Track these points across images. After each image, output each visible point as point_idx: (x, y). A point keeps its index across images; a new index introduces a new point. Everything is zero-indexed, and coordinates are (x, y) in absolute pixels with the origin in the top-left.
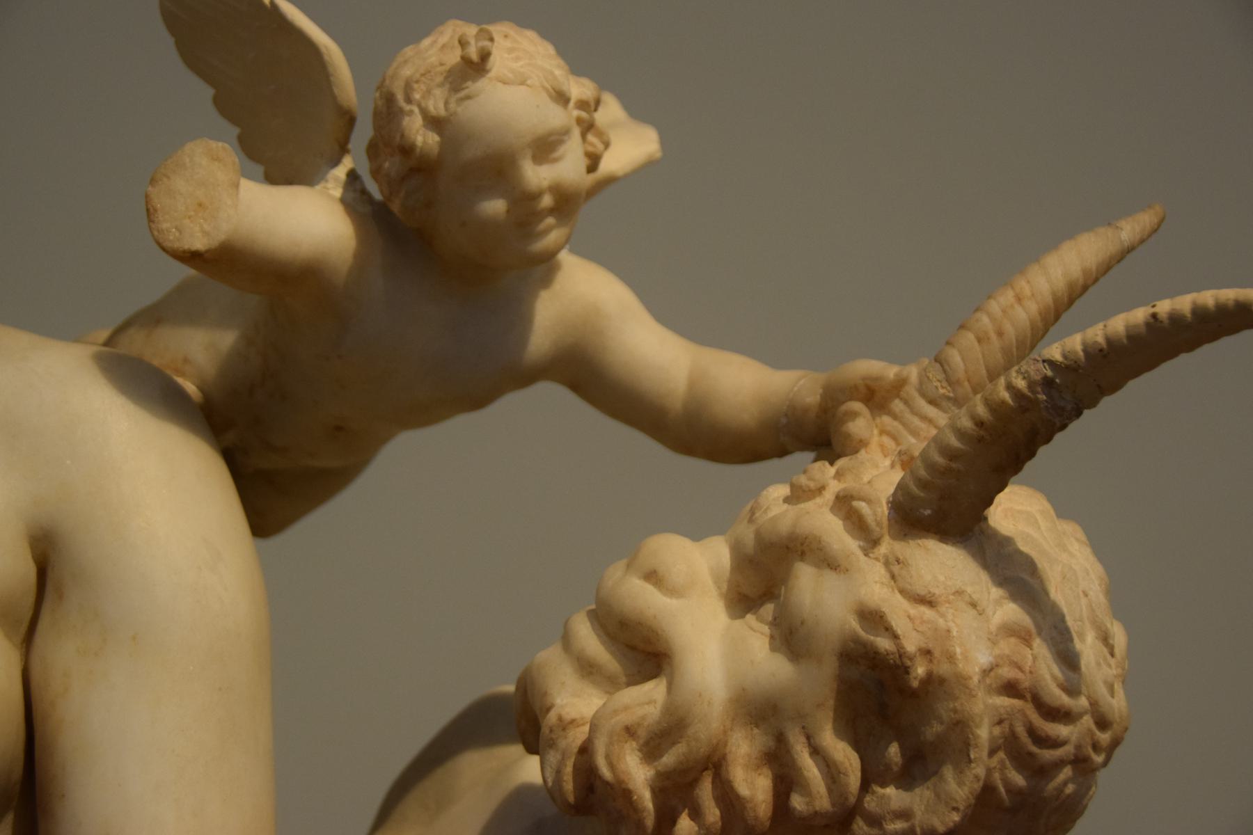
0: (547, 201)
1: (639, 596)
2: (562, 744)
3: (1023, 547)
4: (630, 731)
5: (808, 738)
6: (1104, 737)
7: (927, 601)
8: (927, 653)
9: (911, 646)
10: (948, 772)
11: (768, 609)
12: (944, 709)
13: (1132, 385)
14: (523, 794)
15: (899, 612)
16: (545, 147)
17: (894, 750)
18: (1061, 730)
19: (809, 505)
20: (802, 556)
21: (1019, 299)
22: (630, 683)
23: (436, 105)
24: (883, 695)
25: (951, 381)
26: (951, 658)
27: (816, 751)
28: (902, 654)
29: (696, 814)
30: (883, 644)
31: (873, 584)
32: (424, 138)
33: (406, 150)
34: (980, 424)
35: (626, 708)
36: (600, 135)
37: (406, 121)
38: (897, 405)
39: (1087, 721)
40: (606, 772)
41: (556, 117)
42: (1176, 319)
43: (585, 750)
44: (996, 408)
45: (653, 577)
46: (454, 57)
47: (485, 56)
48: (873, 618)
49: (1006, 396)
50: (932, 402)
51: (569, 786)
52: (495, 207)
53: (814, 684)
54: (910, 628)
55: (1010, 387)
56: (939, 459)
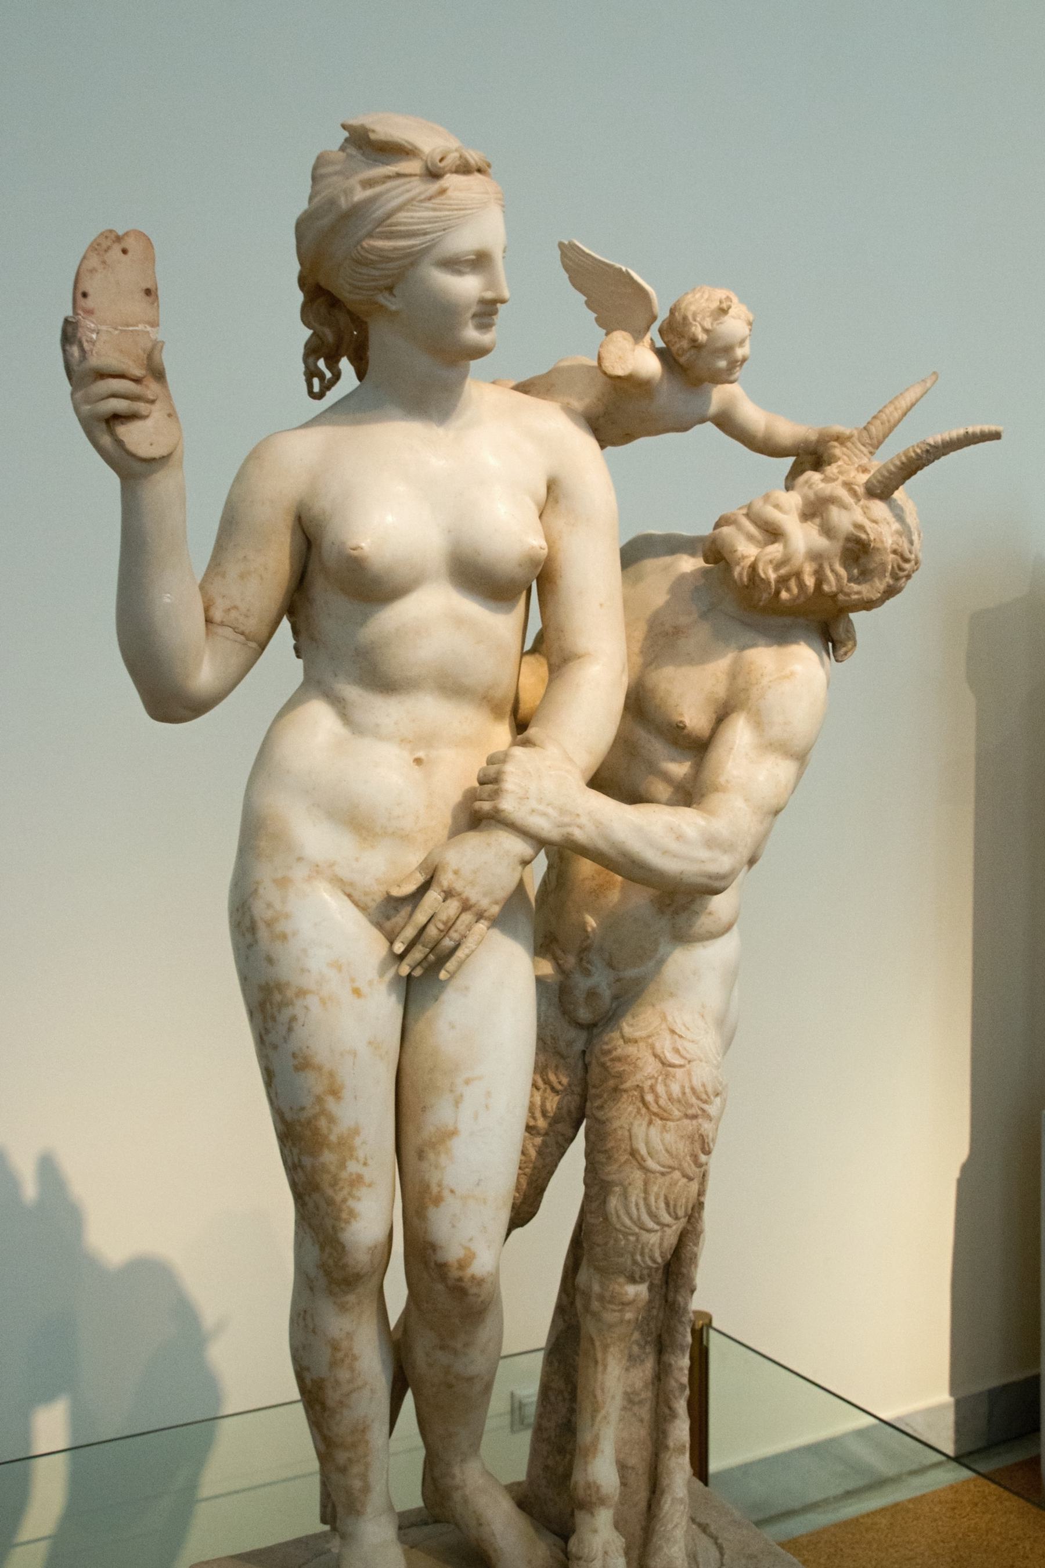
1: (772, 514)
2: (742, 564)
4: (771, 561)
5: (831, 566)
7: (875, 522)
10: (876, 580)
11: (817, 521)
12: (877, 559)
13: (952, 454)
14: (683, 577)
15: (868, 524)
17: (856, 571)
18: (907, 566)
19: (833, 484)
20: (833, 503)
21: (896, 409)
22: (766, 544)
23: (708, 324)
25: (871, 438)
26: (882, 542)
27: (833, 571)
28: (869, 541)
29: (788, 590)
30: (863, 536)
32: (702, 337)
34: (903, 463)
35: (771, 553)
37: (693, 329)
39: (913, 563)
40: (763, 575)
42: (974, 435)
43: (753, 567)
45: (777, 506)
46: (715, 305)
47: (729, 307)
48: (860, 527)
49: (913, 454)
50: (864, 445)
51: (745, 579)
54: (872, 532)
55: (914, 451)
56: (886, 474)
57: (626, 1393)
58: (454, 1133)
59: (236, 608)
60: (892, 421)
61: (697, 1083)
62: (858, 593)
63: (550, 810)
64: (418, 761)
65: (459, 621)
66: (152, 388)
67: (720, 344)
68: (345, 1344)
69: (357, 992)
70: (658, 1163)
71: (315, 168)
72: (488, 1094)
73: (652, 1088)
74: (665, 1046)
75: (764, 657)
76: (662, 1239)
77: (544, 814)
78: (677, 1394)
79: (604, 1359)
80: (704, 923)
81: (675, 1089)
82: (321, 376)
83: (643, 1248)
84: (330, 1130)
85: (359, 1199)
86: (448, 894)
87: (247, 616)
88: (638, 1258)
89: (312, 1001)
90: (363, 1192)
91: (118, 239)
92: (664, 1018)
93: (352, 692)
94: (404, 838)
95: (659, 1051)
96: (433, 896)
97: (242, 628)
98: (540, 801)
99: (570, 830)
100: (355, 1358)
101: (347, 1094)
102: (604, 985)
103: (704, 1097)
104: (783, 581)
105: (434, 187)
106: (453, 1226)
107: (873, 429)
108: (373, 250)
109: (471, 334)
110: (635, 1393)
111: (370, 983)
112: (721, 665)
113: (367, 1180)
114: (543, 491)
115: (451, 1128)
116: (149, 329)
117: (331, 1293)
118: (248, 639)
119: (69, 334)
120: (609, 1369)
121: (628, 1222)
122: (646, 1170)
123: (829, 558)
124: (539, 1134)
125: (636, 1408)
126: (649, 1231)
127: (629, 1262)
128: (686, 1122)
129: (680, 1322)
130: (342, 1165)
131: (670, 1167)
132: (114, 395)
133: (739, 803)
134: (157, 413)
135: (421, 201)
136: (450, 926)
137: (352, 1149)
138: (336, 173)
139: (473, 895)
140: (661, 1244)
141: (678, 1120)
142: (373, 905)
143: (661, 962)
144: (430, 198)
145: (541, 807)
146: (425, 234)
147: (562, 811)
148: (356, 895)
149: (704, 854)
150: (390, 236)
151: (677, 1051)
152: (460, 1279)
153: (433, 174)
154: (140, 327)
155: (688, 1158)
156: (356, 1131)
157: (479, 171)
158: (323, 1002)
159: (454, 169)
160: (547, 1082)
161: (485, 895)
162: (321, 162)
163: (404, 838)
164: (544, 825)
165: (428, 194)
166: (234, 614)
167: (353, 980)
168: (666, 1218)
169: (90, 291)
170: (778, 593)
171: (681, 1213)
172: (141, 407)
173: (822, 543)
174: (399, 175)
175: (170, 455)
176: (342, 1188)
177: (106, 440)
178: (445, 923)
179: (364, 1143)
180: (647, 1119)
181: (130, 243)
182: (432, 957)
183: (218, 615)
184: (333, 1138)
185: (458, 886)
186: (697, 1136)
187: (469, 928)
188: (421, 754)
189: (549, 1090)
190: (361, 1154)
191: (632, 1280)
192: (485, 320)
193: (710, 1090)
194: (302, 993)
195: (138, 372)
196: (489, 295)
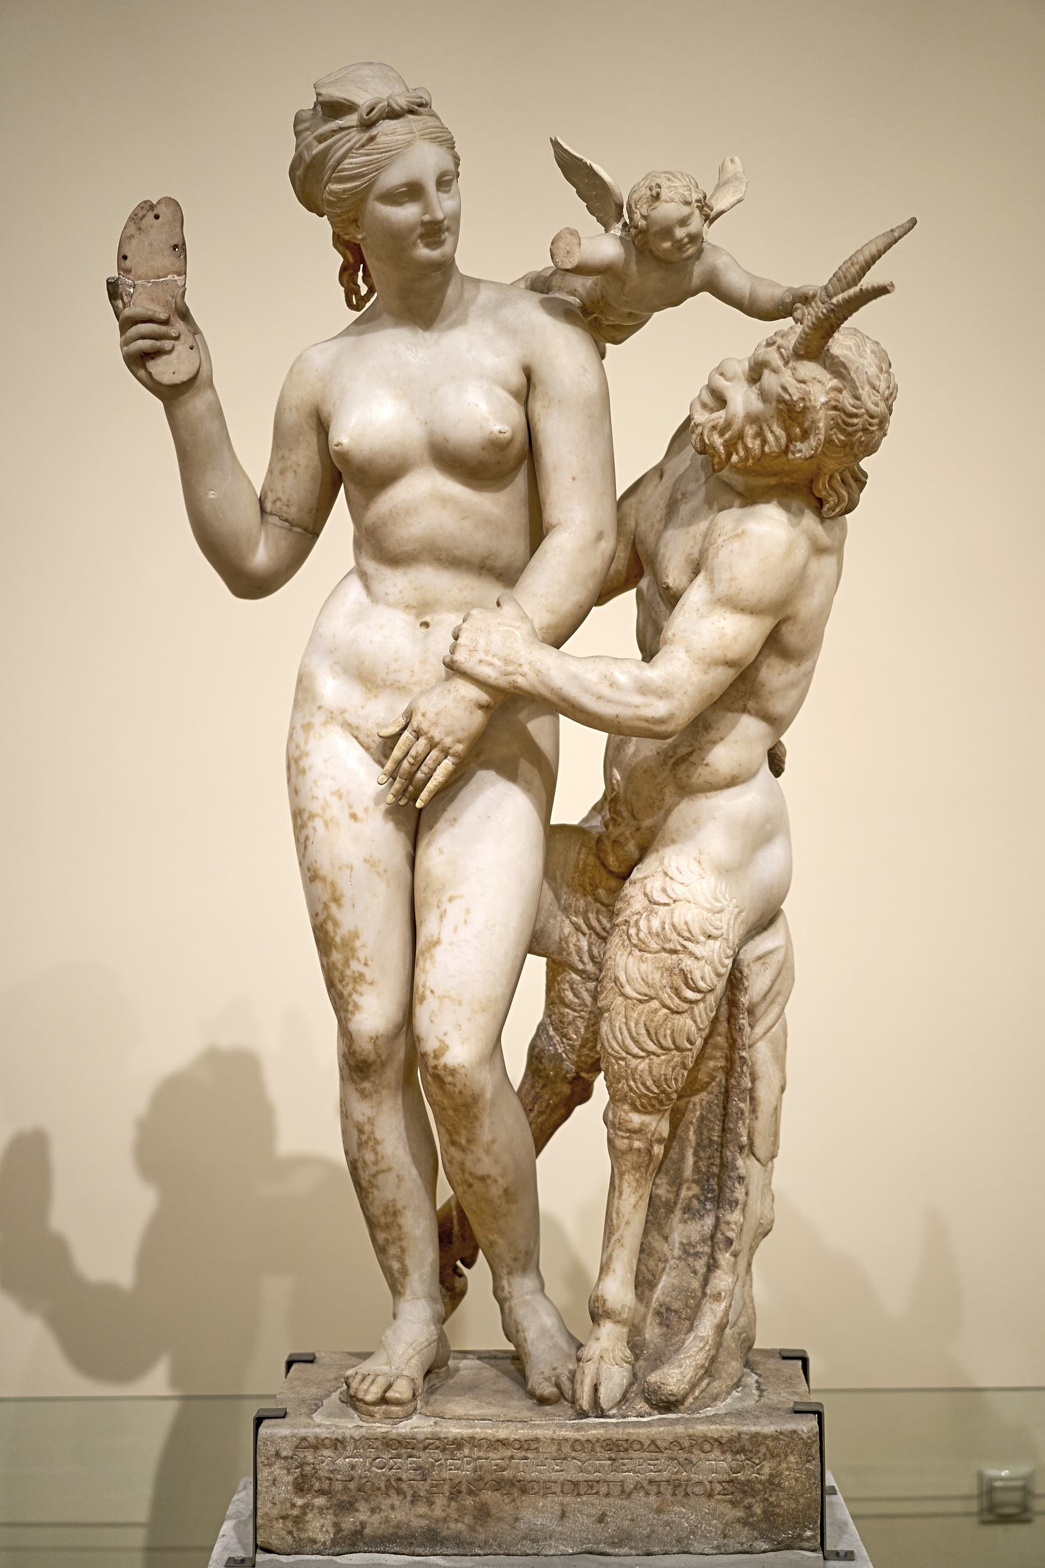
0: (686, 240)
3: (842, 359)
4: (714, 428)
6: (876, 421)
7: (803, 382)
8: (803, 399)
9: (795, 398)
10: (812, 437)
12: (809, 417)
16: (683, 222)
18: (855, 421)
21: (852, 264)
23: (644, 212)
24: (792, 413)
26: (810, 400)
27: (772, 432)
29: (737, 454)
30: (787, 397)
31: (787, 378)
32: (642, 223)
33: (636, 227)
36: (708, 207)
38: (813, 304)
39: (866, 417)
40: (707, 441)
41: (686, 210)
43: (702, 434)
44: (818, 318)
45: (722, 374)
46: (649, 193)
47: (658, 194)
48: (784, 389)
52: (667, 245)
57: (681, 1243)
58: (437, 943)
59: (279, 499)
60: (849, 276)
61: (676, 920)
62: (800, 451)
63: (495, 661)
64: (426, 625)
65: (445, 501)
67: (654, 229)
68: (367, 1128)
69: (354, 817)
70: (635, 990)
71: (295, 126)
72: (468, 911)
73: (637, 922)
74: (655, 886)
75: (728, 520)
77: (490, 664)
78: (721, 1246)
79: (620, 1186)
80: (700, 775)
81: (656, 924)
82: (357, 292)
83: (633, 1075)
84: (335, 932)
85: (362, 995)
86: (418, 734)
87: (288, 506)
88: (632, 1083)
89: (318, 823)
90: (364, 988)
91: (152, 207)
92: (662, 863)
93: (371, 566)
94: (400, 688)
95: (648, 891)
96: (406, 733)
97: (286, 516)
98: (487, 653)
99: (514, 678)
100: (377, 1142)
101: (346, 901)
102: (628, 833)
103: (687, 934)
104: (730, 447)
105: (366, 136)
106: (432, 1021)
107: (830, 287)
108: (331, 193)
109: (423, 252)
110: (690, 1244)
111: (366, 810)
112: (703, 526)
113: (369, 977)
114: (517, 379)
115: (435, 938)
116: (176, 278)
117: (354, 1082)
118: (292, 524)
119: (114, 290)
120: (624, 1196)
121: (617, 1048)
122: (626, 997)
123: (766, 420)
124: (590, 978)
125: (690, 1259)
126: (635, 1056)
127: (626, 1088)
128: (665, 955)
129: (730, 1177)
130: (346, 963)
131: (646, 995)
132: (143, 337)
133: (682, 655)
134: (181, 347)
135: (358, 149)
136: (419, 762)
137: (353, 950)
138: (307, 129)
139: (437, 734)
140: (650, 1072)
141: (657, 952)
142: (374, 746)
143: (668, 812)
144: (363, 146)
145: (489, 658)
146: (364, 176)
147: (507, 662)
148: (361, 737)
150: (341, 180)
151: (664, 890)
152: (435, 1067)
153: (367, 125)
154: (170, 277)
156: (355, 935)
157: (412, 112)
158: (326, 824)
159: (384, 115)
160: (591, 927)
161: (447, 734)
162: (298, 121)
163: (400, 688)
164: (489, 673)
165: (361, 142)
166: (278, 503)
167: (351, 807)
168: (652, 1047)
169: (129, 255)
170: (729, 456)
171: (668, 1043)
172: (167, 344)
173: (757, 405)
174: (342, 129)
176: (348, 984)
177: (142, 373)
178: (415, 758)
179: (364, 946)
180: (629, 950)
181: (162, 210)
182: (411, 788)
183: (269, 506)
184: (338, 939)
185: (425, 726)
186: (677, 971)
188: (427, 619)
189: (594, 936)
190: (361, 955)
191: (635, 1109)
192: (431, 240)
193: (696, 930)
194: (312, 816)
195: (163, 316)
196: (427, 218)
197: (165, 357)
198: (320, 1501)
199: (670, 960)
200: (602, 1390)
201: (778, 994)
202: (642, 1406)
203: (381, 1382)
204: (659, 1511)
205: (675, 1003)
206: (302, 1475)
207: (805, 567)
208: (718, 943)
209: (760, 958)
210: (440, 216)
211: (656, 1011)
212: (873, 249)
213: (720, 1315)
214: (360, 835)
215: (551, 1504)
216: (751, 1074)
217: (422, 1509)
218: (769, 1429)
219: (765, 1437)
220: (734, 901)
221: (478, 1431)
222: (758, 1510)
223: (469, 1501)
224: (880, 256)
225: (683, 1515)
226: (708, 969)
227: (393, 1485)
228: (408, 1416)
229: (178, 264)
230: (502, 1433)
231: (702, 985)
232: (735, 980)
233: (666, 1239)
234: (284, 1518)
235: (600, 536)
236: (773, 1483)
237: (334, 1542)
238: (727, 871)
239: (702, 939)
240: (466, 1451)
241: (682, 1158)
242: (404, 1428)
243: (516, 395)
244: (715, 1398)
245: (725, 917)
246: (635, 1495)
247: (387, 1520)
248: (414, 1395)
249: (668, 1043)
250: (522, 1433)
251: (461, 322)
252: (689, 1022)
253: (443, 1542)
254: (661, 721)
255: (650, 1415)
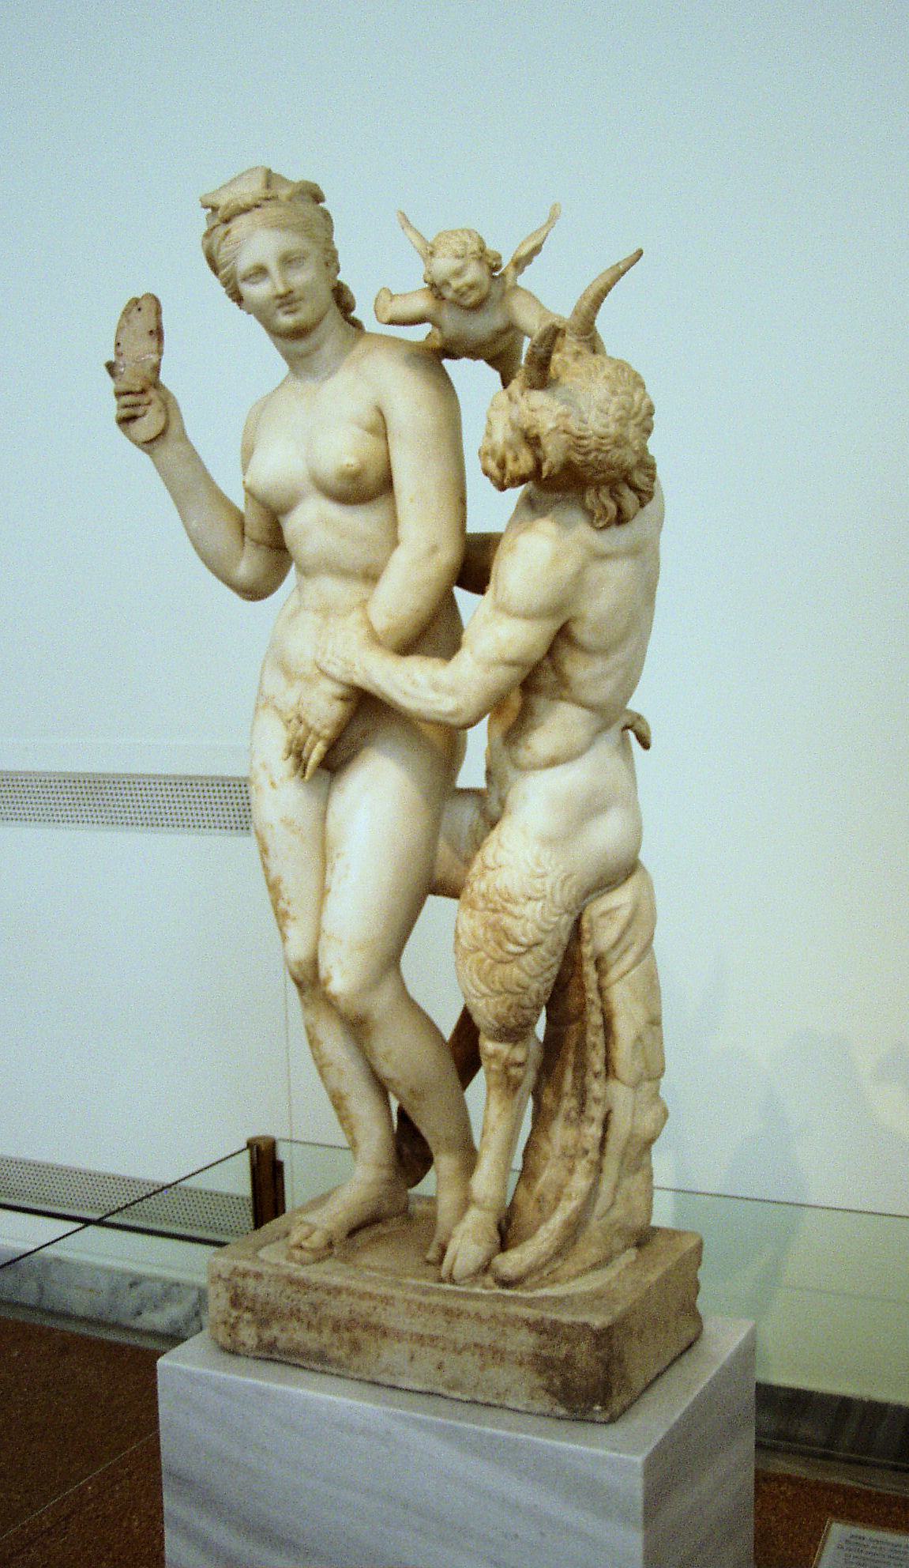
16: (458, 273)
18: (585, 442)
41: (458, 263)
53: (516, 438)
61: (498, 883)
66: (152, 394)
69: (273, 784)
76: (487, 1005)
90: (289, 922)
101: (271, 853)
114: (370, 417)
119: (111, 367)
134: (152, 411)
139: (311, 720)
149: (432, 696)
153: (227, 221)
155: (492, 943)
157: (258, 206)
168: (483, 988)
171: (498, 986)
172: (140, 411)
175: (163, 433)
181: (144, 304)
187: (314, 746)
190: (286, 896)
193: (516, 891)
195: (138, 389)
197: (139, 421)
198: (247, 1316)
199: (493, 917)
200: (458, 1264)
201: (632, 944)
202: (489, 1280)
203: (305, 1229)
204: (482, 1368)
205: (500, 954)
206: (236, 1295)
207: (579, 575)
208: (540, 904)
209: (604, 914)
210: (281, 290)
211: (482, 961)
212: (601, 284)
213: (568, 1212)
214: (280, 797)
215: (405, 1347)
216: (603, 1012)
217: (313, 1334)
218: (566, 1318)
219: (563, 1325)
220: (561, 867)
221: (353, 1284)
222: (557, 1382)
223: (346, 1335)
224: (609, 289)
225: (503, 1376)
226: (529, 925)
227: (295, 1314)
228: (319, 1260)
229: (154, 344)
230: (369, 1288)
231: (524, 940)
232: (577, 932)
233: (549, 1140)
234: (225, 1323)
235: (434, 549)
236: (568, 1362)
237: (258, 1348)
238: (549, 841)
239: (522, 900)
240: (344, 1296)
241: (563, 1073)
242: (302, 1273)
243: (372, 430)
244: (555, 1281)
245: (548, 881)
246: (467, 1354)
247: (291, 1340)
248: (330, 1245)
249: (498, 986)
250: (383, 1290)
251: (331, 374)
252: (516, 971)
253: (329, 1362)
254: (451, 714)
255: (491, 1288)
